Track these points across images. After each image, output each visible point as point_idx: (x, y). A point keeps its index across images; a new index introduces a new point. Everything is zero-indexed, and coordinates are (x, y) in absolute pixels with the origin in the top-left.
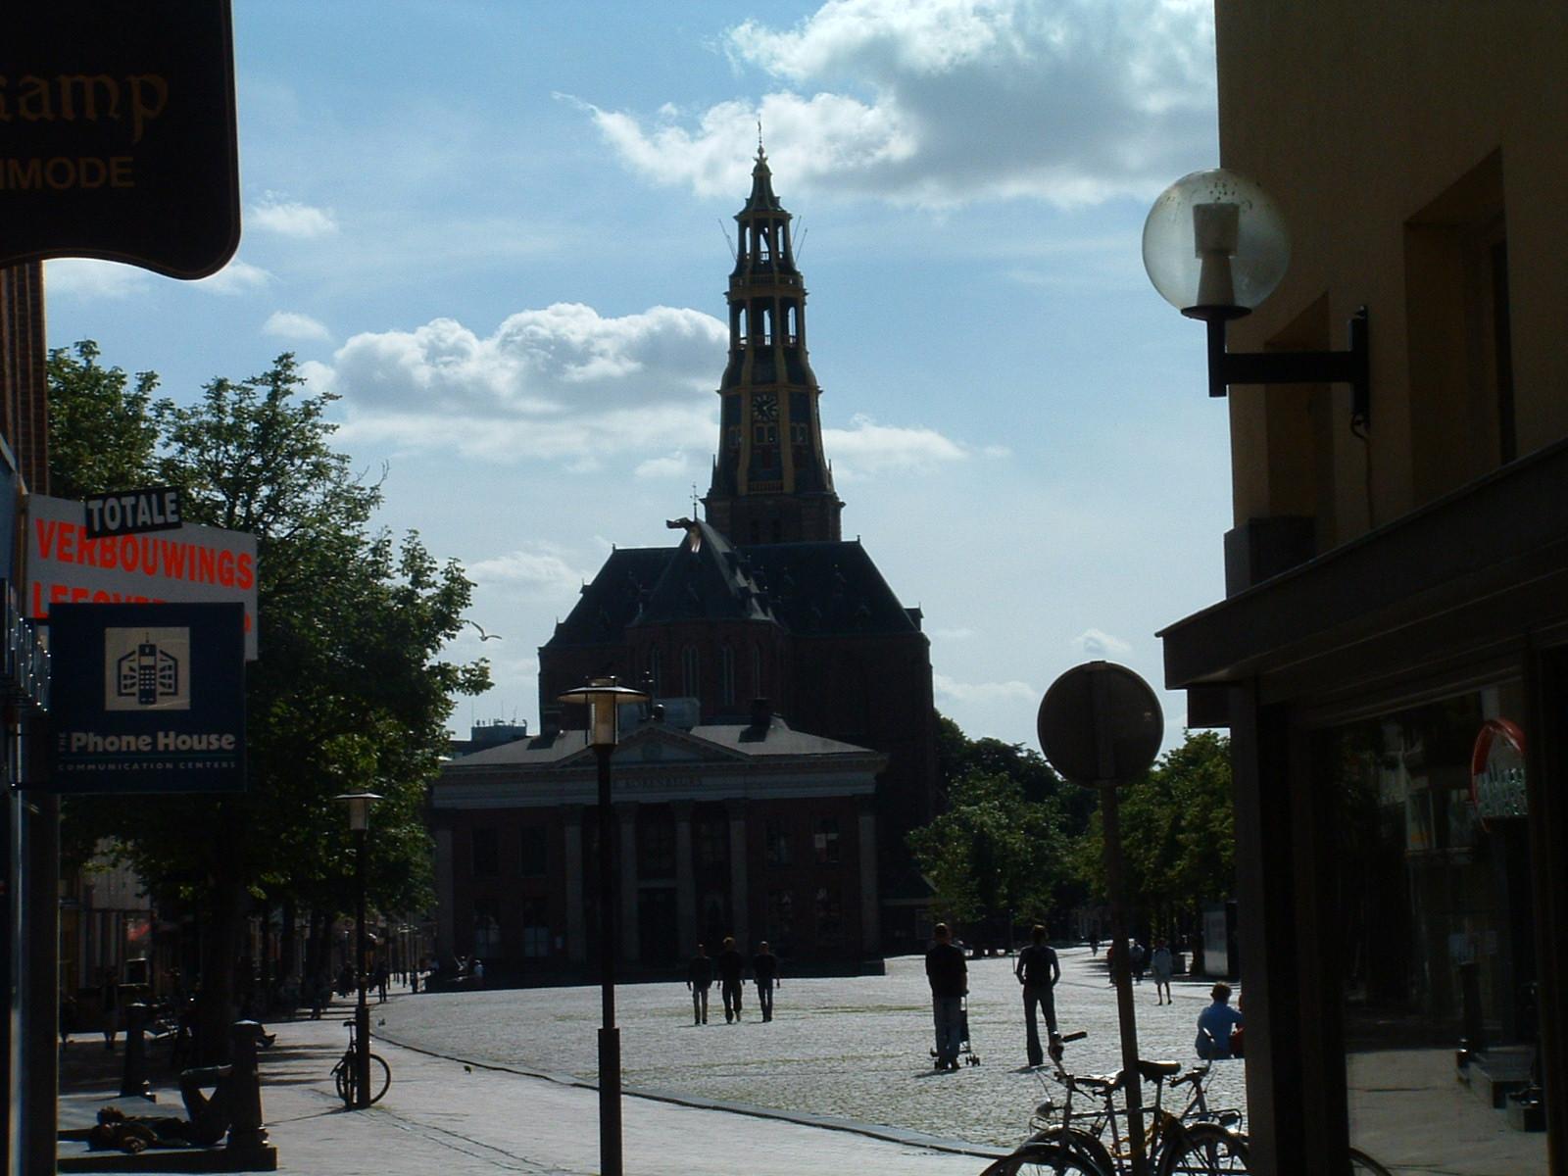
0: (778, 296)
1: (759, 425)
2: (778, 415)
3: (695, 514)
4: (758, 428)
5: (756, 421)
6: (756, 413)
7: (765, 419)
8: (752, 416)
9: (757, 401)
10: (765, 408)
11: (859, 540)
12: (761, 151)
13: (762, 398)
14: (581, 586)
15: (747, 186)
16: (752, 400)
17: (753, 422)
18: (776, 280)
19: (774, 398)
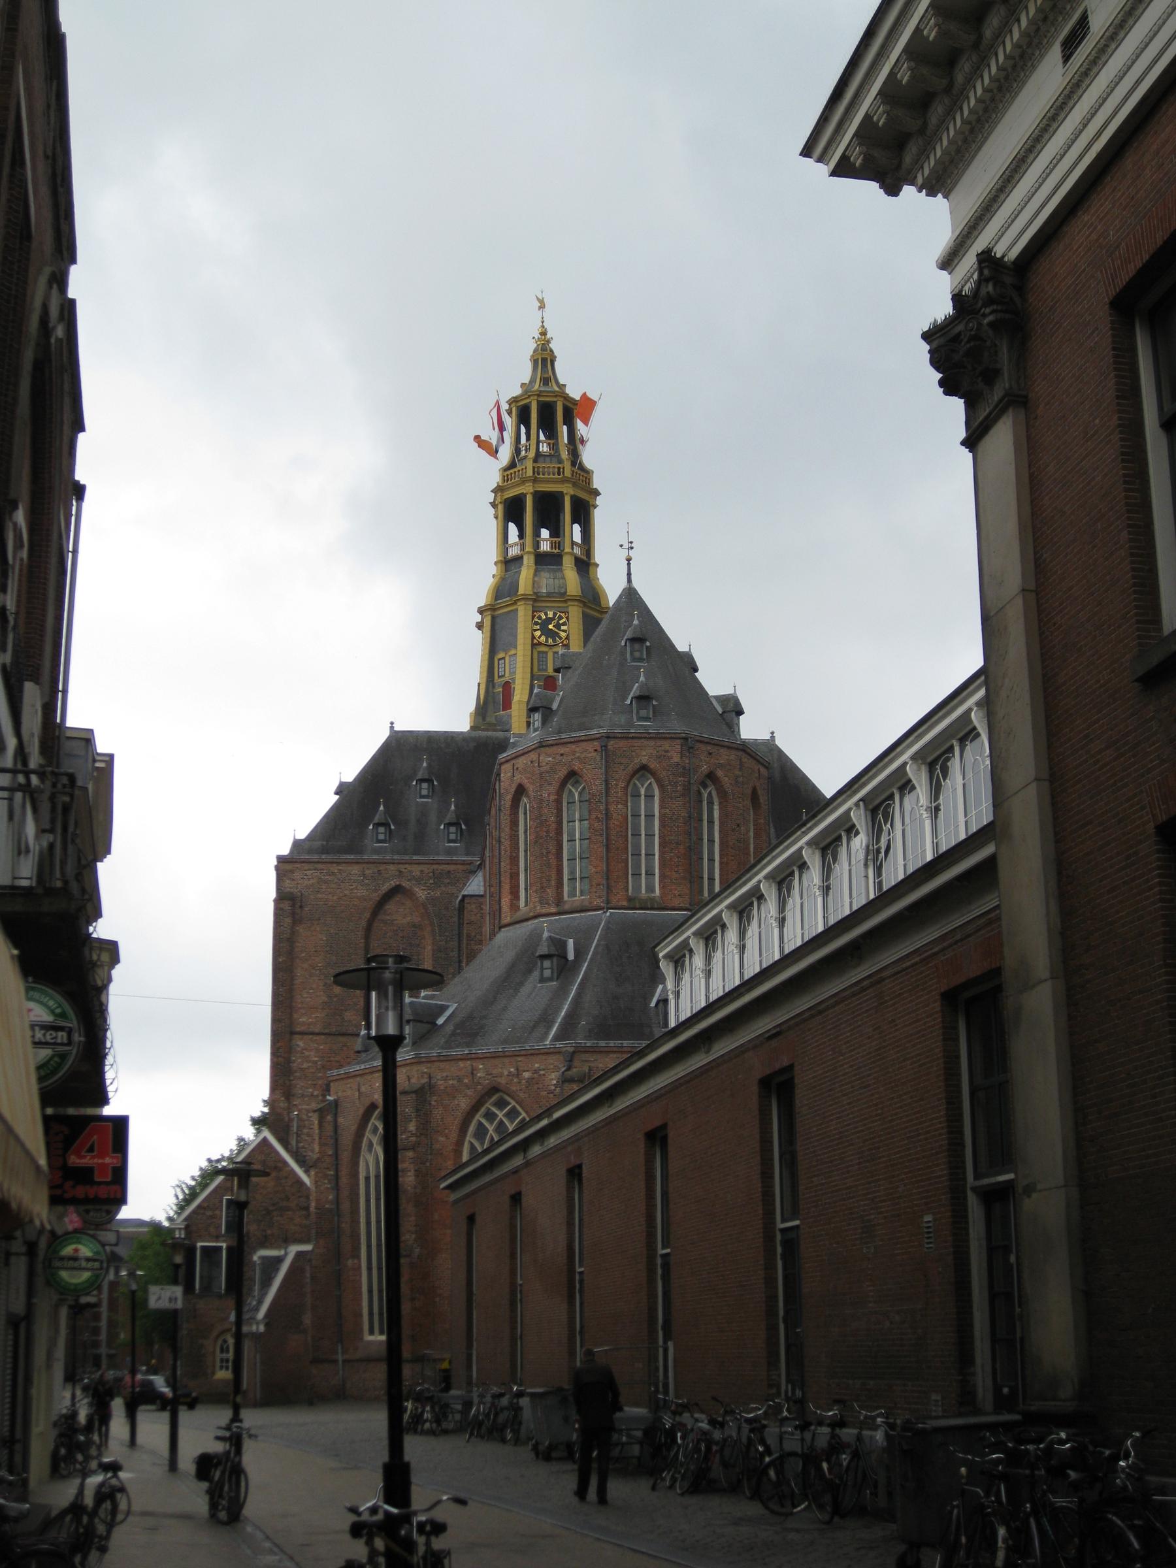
0: (568, 491)
1: (543, 649)
2: (567, 638)
3: (629, 574)
4: (539, 652)
5: (540, 644)
6: (538, 633)
7: (550, 640)
8: (533, 637)
9: (540, 618)
10: (551, 627)
11: (773, 737)
12: (544, 333)
13: (546, 614)
14: (337, 784)
15: (525, 373)
16: (533, 617)
17: (533, 645)
18: (568, 473)
19: (563, 615)
